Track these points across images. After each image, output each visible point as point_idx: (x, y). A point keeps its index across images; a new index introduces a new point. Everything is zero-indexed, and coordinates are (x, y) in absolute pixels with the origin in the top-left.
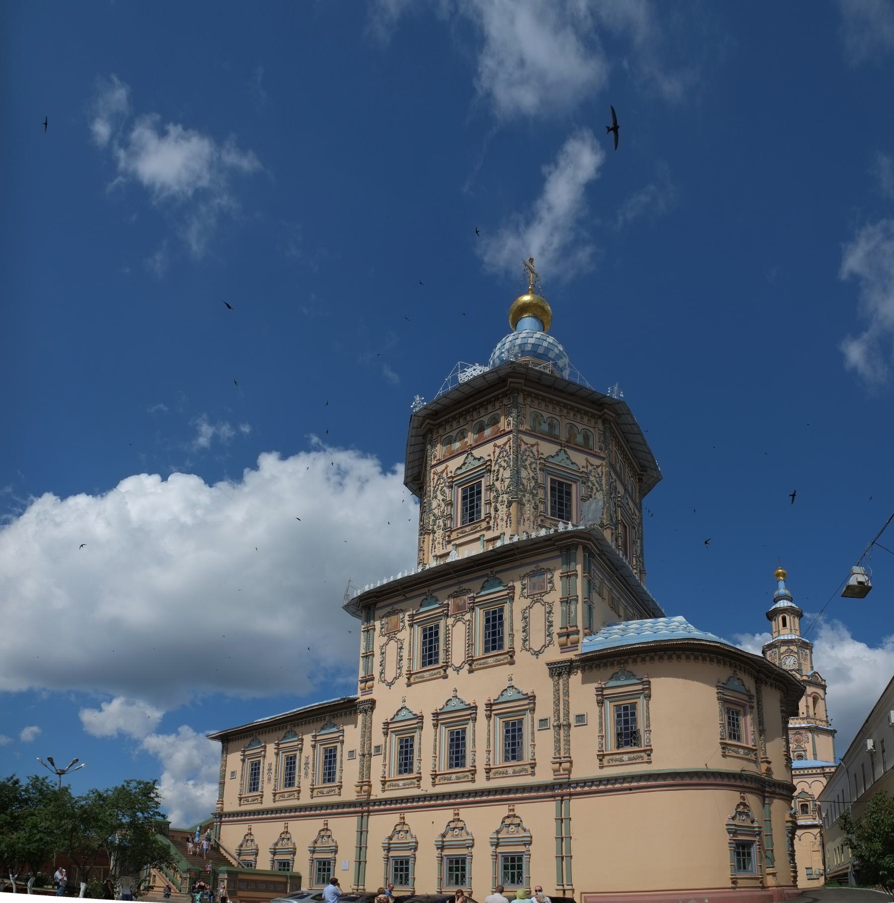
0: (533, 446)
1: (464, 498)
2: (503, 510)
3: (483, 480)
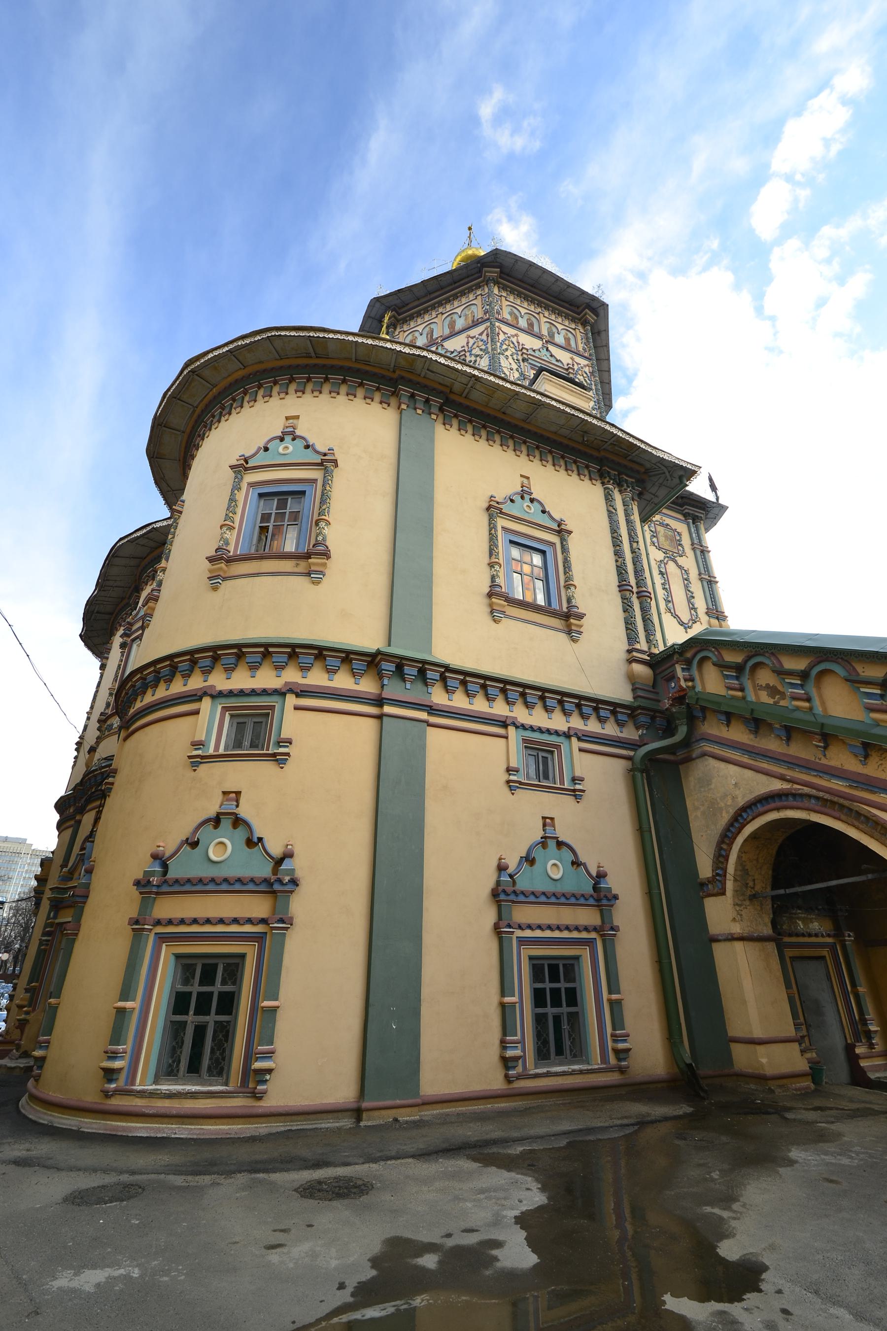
0: (513, 336)
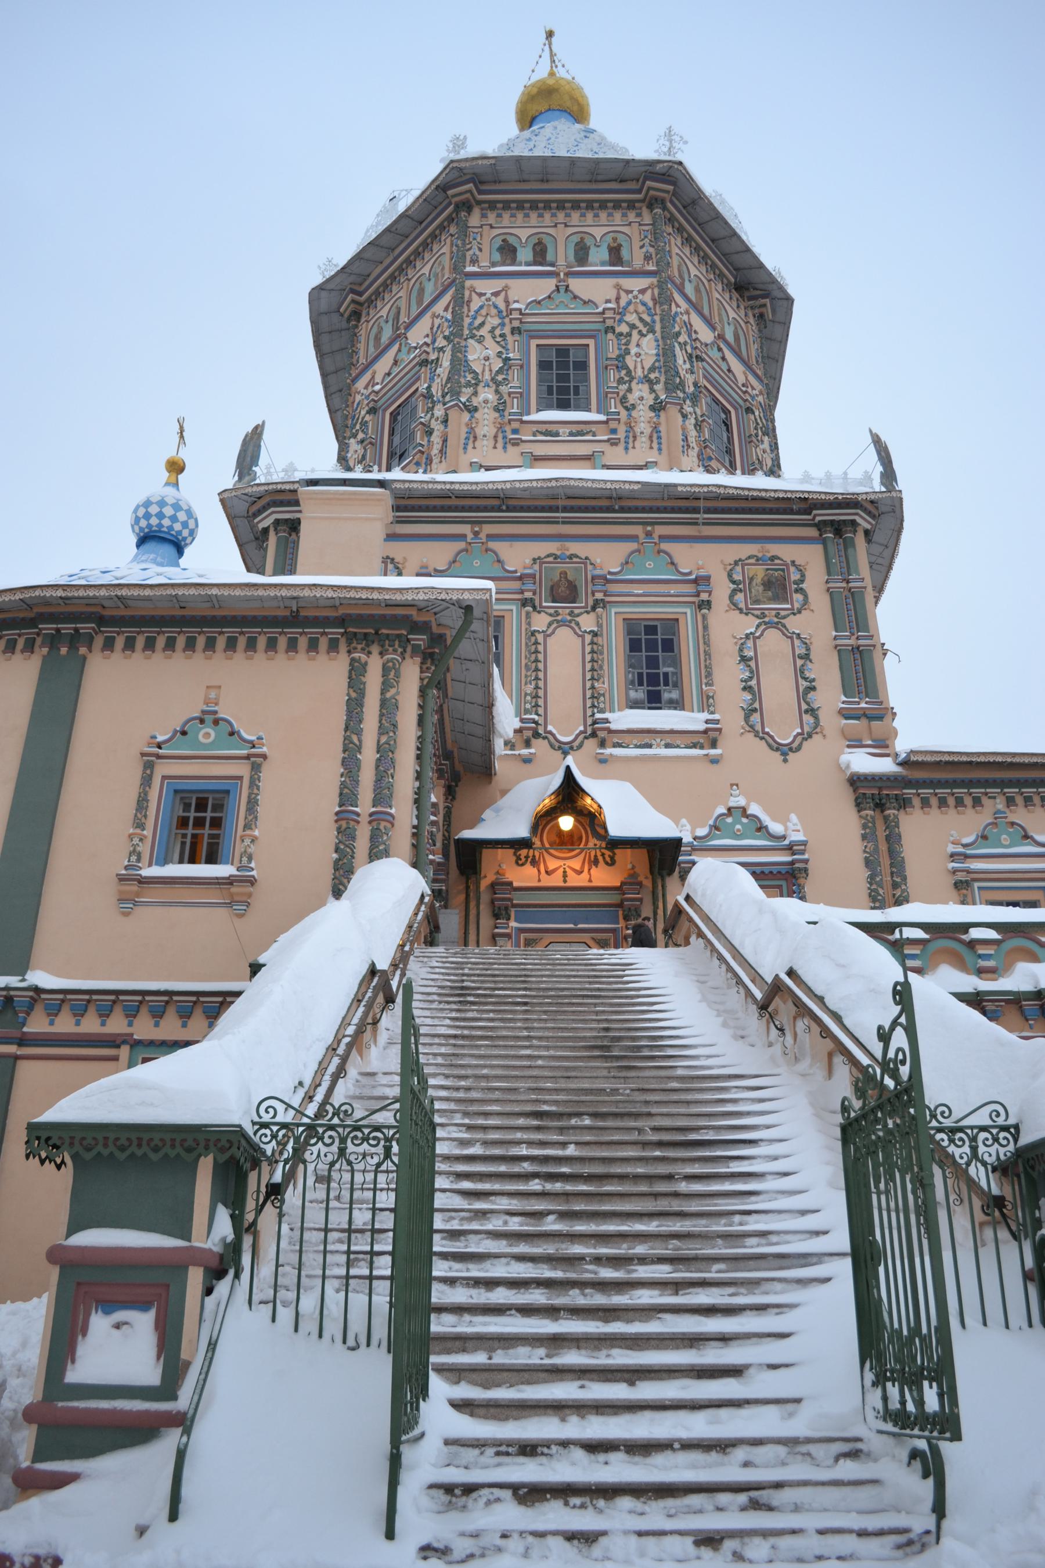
1: (543, 365)
2: (643, 415)
3: (591, 342)
